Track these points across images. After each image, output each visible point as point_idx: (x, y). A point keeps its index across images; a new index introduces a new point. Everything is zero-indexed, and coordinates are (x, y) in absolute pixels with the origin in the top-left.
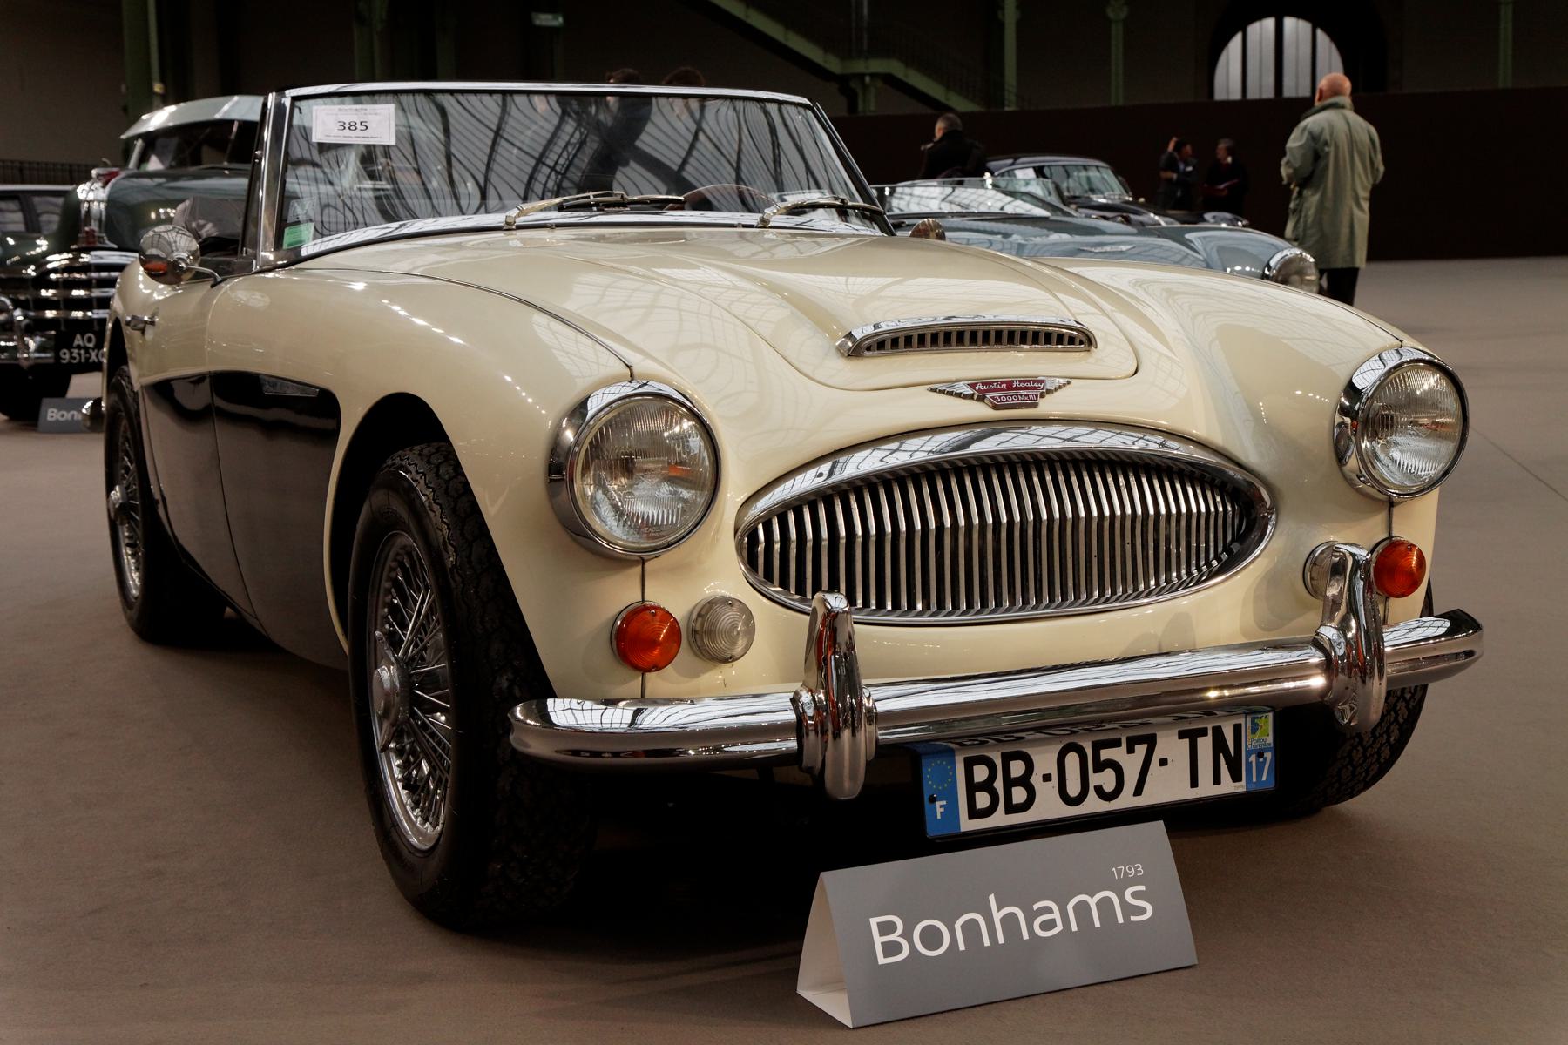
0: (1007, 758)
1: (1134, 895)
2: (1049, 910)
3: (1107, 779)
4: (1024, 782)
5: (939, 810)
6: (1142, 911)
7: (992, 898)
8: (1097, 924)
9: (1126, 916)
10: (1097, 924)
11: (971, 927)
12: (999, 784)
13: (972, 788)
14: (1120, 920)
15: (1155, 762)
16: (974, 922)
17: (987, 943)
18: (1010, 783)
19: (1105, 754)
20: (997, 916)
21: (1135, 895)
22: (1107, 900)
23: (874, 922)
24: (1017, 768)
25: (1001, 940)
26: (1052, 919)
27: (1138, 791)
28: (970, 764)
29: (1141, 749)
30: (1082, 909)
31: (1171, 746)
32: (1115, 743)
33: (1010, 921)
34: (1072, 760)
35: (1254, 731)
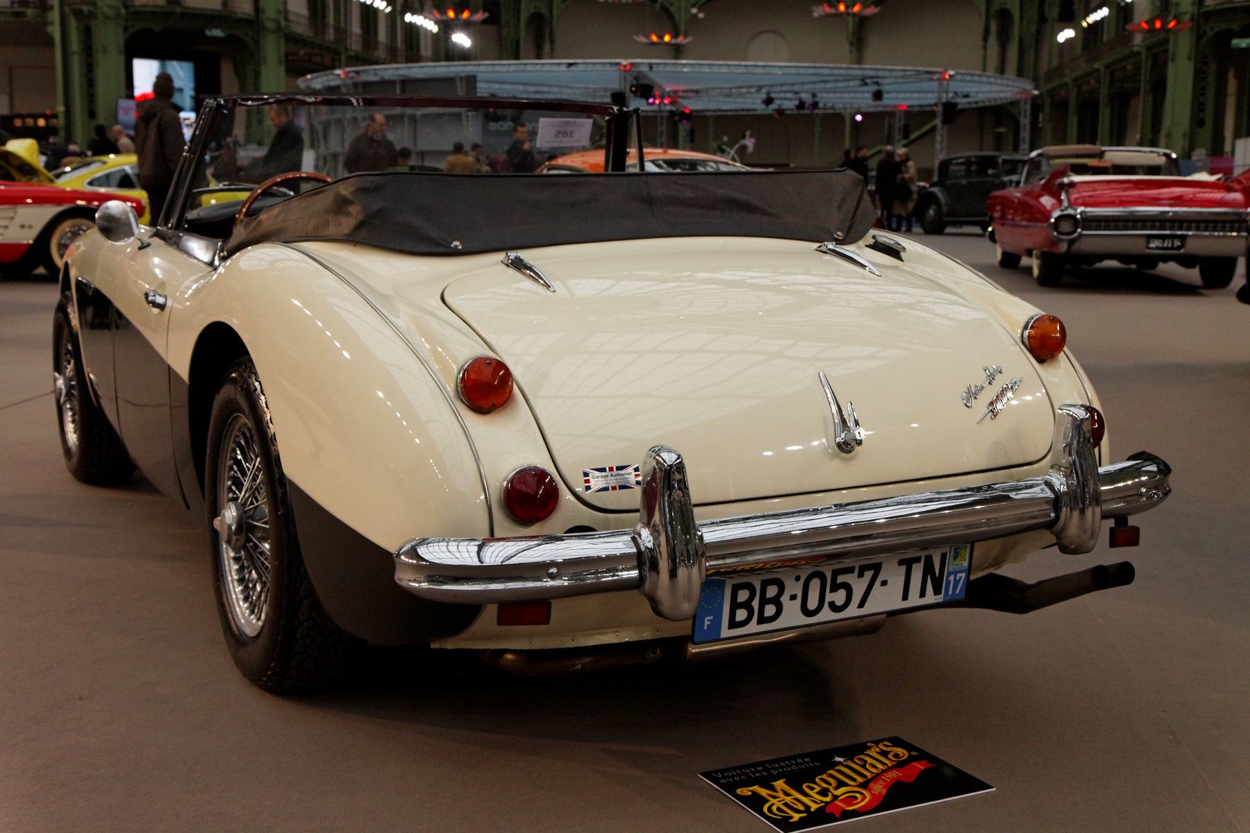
0: (765, 584)
3: (839, 597)
4: (776, 601)
5: (707, 623)
12: (755, 604)
13: (735, 606)
15: (878, 583)
18: (764, 602)
19: (841, 579)
24: (772, 591)
27: (861, 605)
28: (736, 589)
29: (869, 574)
31: (894, 575)
32: (850, 570)
34: (815, 585)
35: (955, 558)
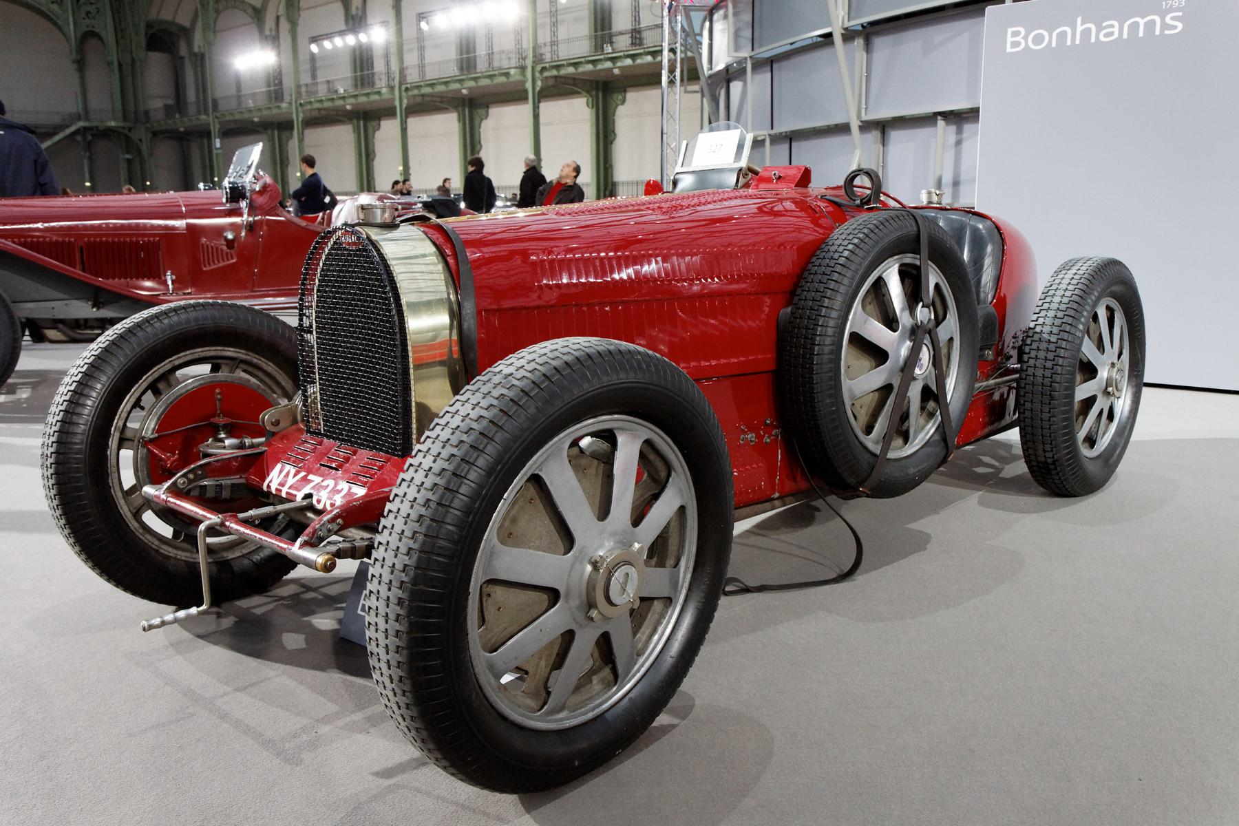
1: (1172, 18)
2: (1112, 26)
7: (1079, 19)
8: (1141, 34)
9: (1162, 30)
10: (1141, 34)
14: (1157, 32)
16: (1065, 32)
17: (1069, 43)
20: (1079, 28)
22: (1153, 22)
25: (1078, 42)
33: (1086, 33)
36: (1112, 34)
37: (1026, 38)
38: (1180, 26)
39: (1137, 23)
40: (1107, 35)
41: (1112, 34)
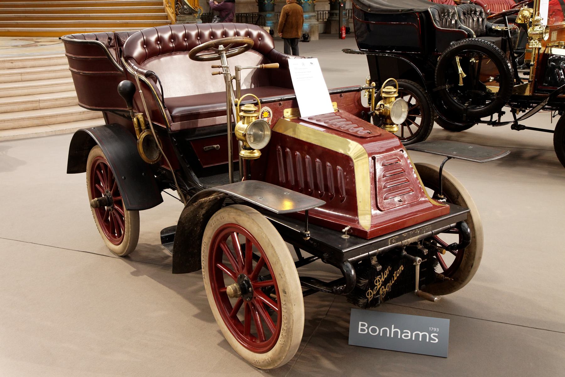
1: (434, 336)
6: (435, 340)
7: (393, 326)
8: (420, 340)
10: (420, 340)
11: (385, 331)
14: (427, 341)
17: (388, 336)
20: (393, 330)
21: (434, 336)
22: (426, 335)
23: (360, 323)
25: (392, 336)
26: (408, 335)
30: (417, 335)
33: (396, 333)
36: (408, 336)
37: (368, 328)
38: (437, 340)
39: (419, 334)
40: (405, 336)
41: (408, 336)
